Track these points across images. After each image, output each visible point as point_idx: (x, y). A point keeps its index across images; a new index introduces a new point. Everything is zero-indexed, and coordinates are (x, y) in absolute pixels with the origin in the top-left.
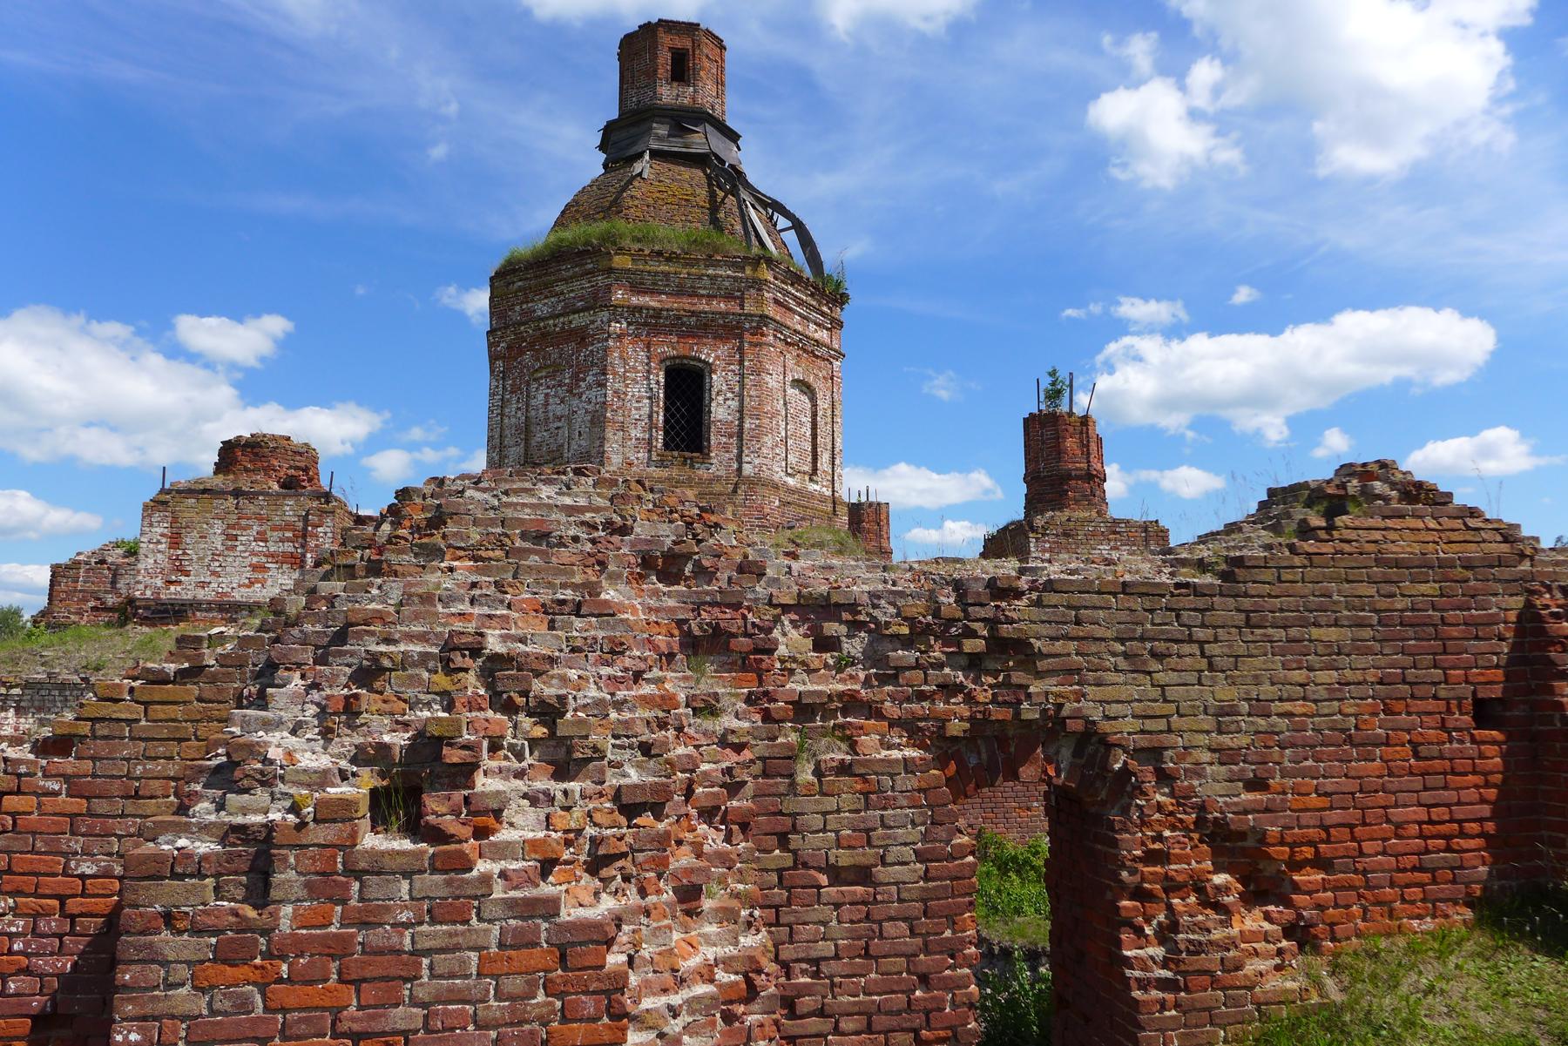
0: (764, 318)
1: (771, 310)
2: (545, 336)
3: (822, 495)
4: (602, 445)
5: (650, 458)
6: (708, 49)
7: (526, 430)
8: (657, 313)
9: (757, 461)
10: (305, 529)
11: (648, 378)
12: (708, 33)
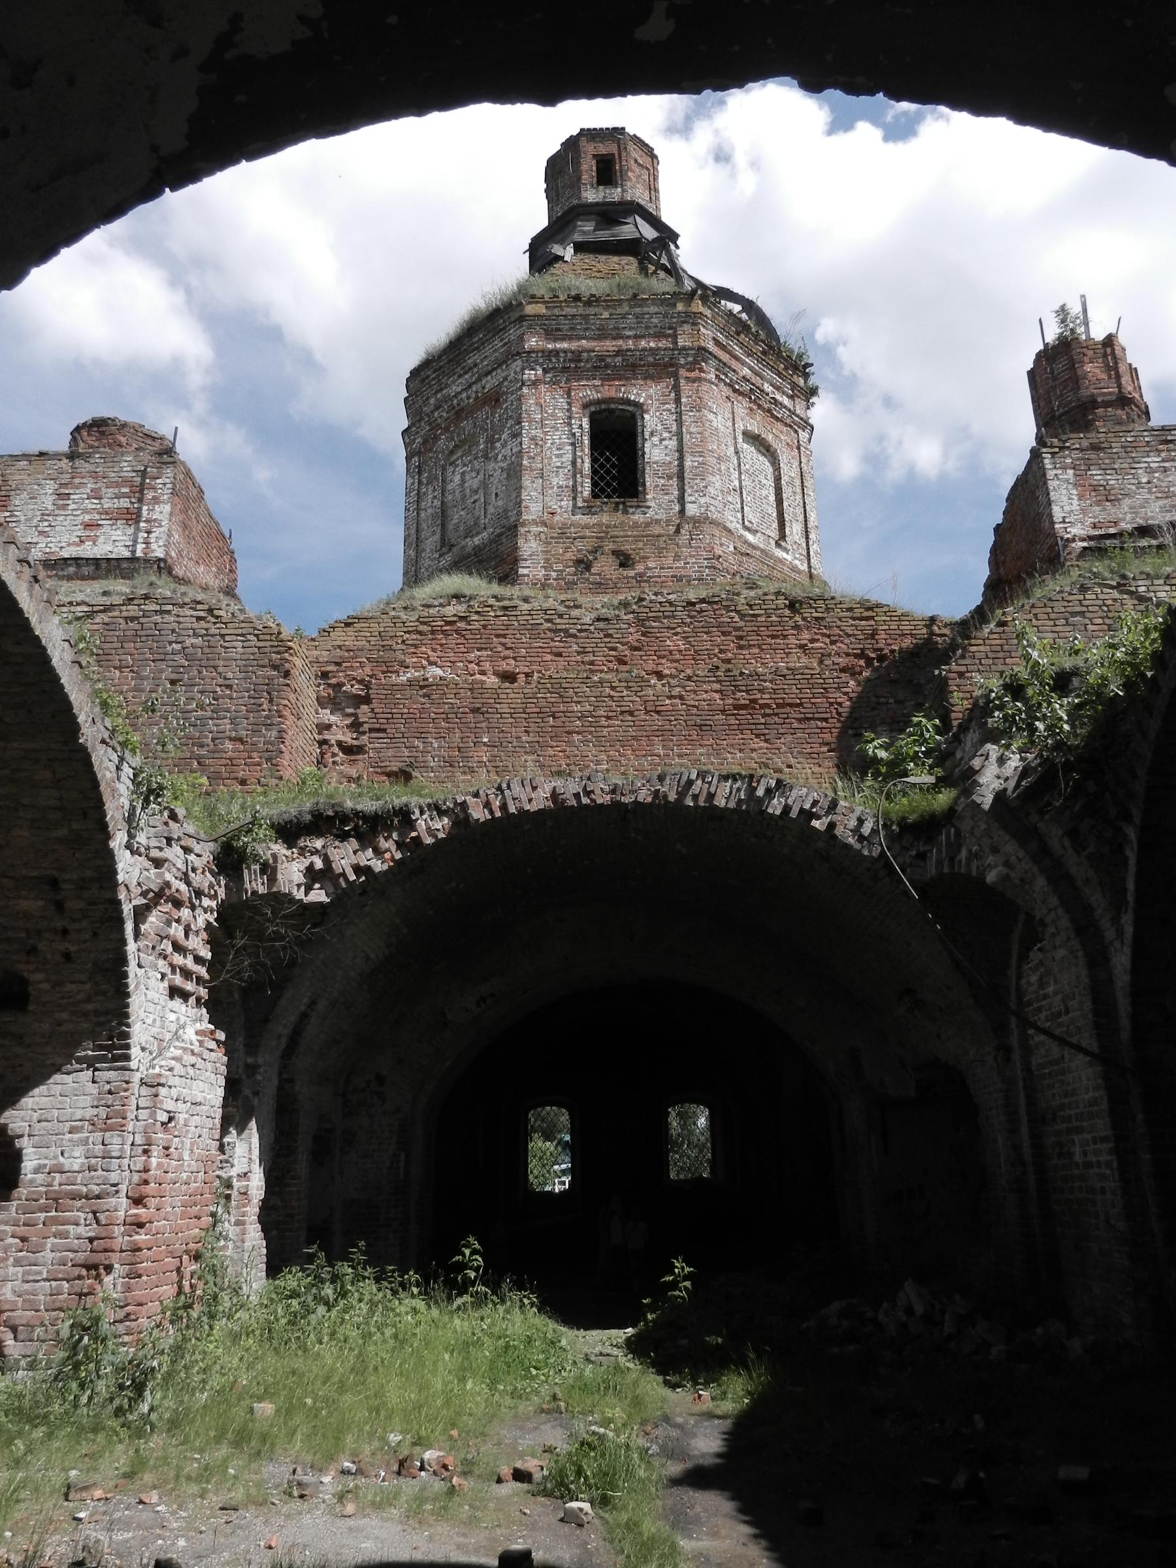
0: (702, 353)
1: (711, 346)
2: (459, 414)
3: (794, 569)
4: (519, 495)
5: (575, 506)
6: (634, 152)
7: (443, 514)
8: (577, 356)
9: (703, 500)
10: (142, 484)
11: (570, 424)
12: (636, 139)
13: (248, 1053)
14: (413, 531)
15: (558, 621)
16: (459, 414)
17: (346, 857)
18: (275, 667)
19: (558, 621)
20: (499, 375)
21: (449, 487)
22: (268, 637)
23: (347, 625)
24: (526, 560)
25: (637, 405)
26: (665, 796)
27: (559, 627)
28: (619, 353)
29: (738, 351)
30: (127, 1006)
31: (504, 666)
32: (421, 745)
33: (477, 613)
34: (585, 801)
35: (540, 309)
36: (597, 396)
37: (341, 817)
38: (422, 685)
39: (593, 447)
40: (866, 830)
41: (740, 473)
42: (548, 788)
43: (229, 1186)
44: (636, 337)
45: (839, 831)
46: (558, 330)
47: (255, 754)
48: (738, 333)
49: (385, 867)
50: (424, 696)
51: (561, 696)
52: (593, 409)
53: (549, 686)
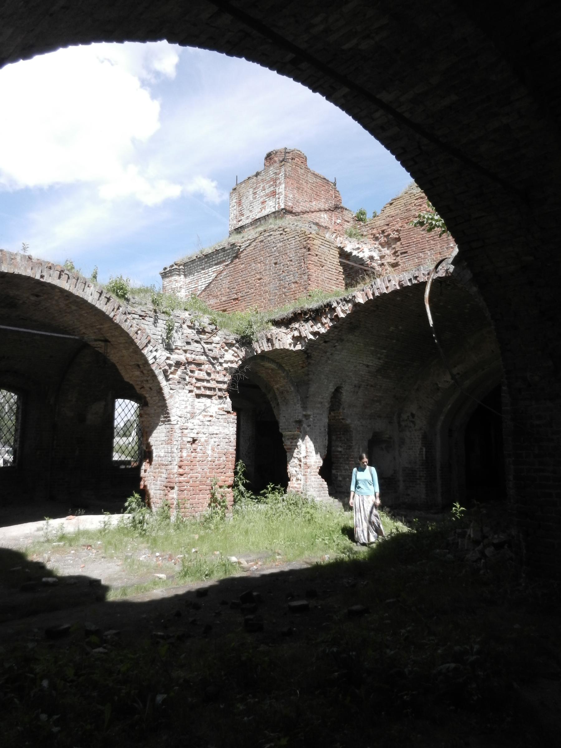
13: (304, 411)
17: (307, 330)
18: (305, 248)
22: (302, 235)
23: (391, 204)
30: (166, 404)
32: (423, 256)
34: (415, 282)
37: (305, 313)
42: (397, 279)
43: (300, 461)
47: (301, 287)
49: (326, 330)
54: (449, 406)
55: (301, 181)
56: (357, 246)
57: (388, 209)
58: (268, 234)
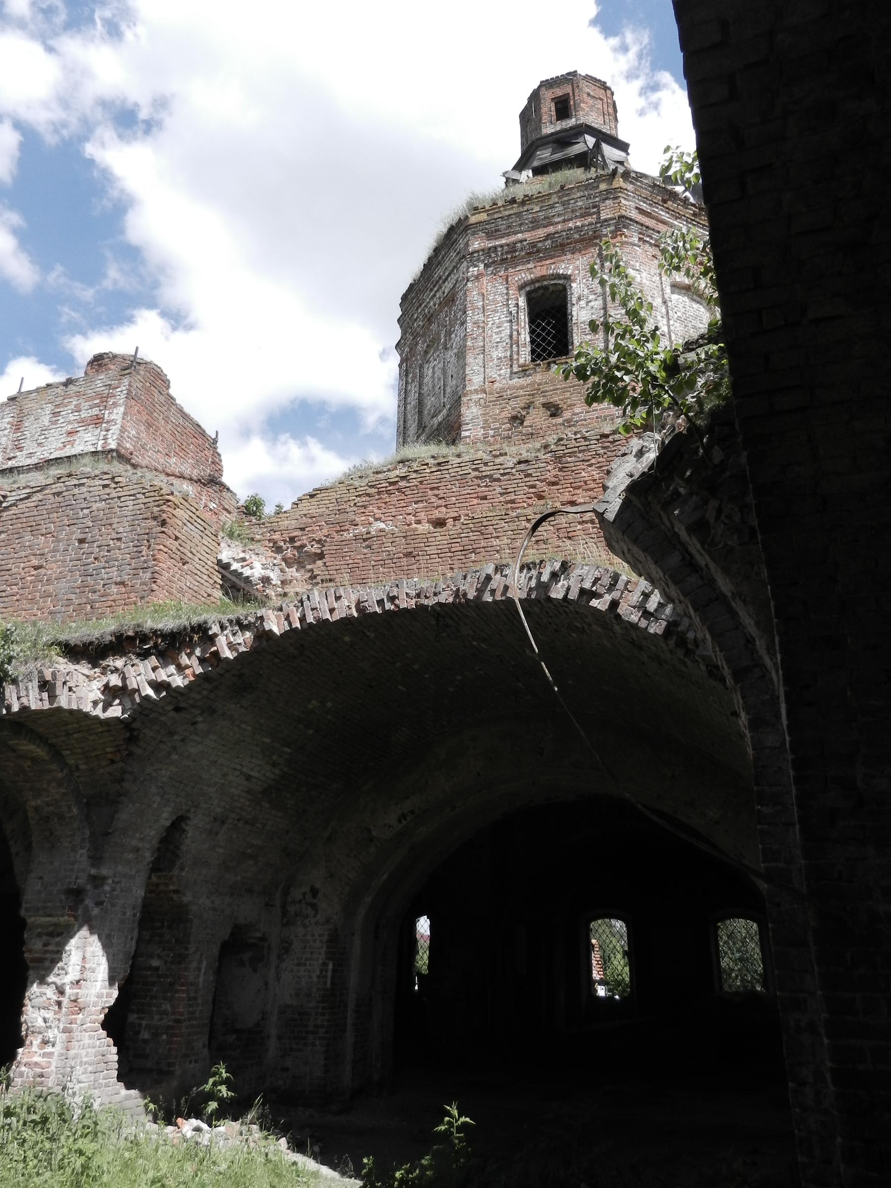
0: (623, 221)
1: (634, 214)
4: (464, 370)
5: (512, 373)
11: (508, 305)
13: (93, 866)
14: (402, 423)
15: (484, 468)
16: (430, 319)
17: (142, 675)
18: (155, 518)
19: (484, 468)
20: (453, 277)
21: (425, 381)
22: (152, 494)
24: (468, 424)
25: (567, 278)
26: (465, 595)
27: (484, 474)
28: (548, 237)
29: (664, 216)
31: (437, 514)
33: (416, 471)
34: (388, 606)
35: (483, 217)
36: (529, 277)
37: (142, 637)
38: (366, 539)
39: (532, 321)
40: (652, 605)
41: (669, 320)
42: (354, 598)
43: (61, 992)
44: (564, 221)
45: (622, 610)
46: (498, 230)
47: (132, 595)
48: (665, 201)
49: (186, 682)
50: (369, 547)
51: (482, 534)
52: (528, 289)
53: (471, 526)
54: (385, 877)
55: (155, 414)
56: (242, 555)
57: (305, 503)
58: (77, 482)
